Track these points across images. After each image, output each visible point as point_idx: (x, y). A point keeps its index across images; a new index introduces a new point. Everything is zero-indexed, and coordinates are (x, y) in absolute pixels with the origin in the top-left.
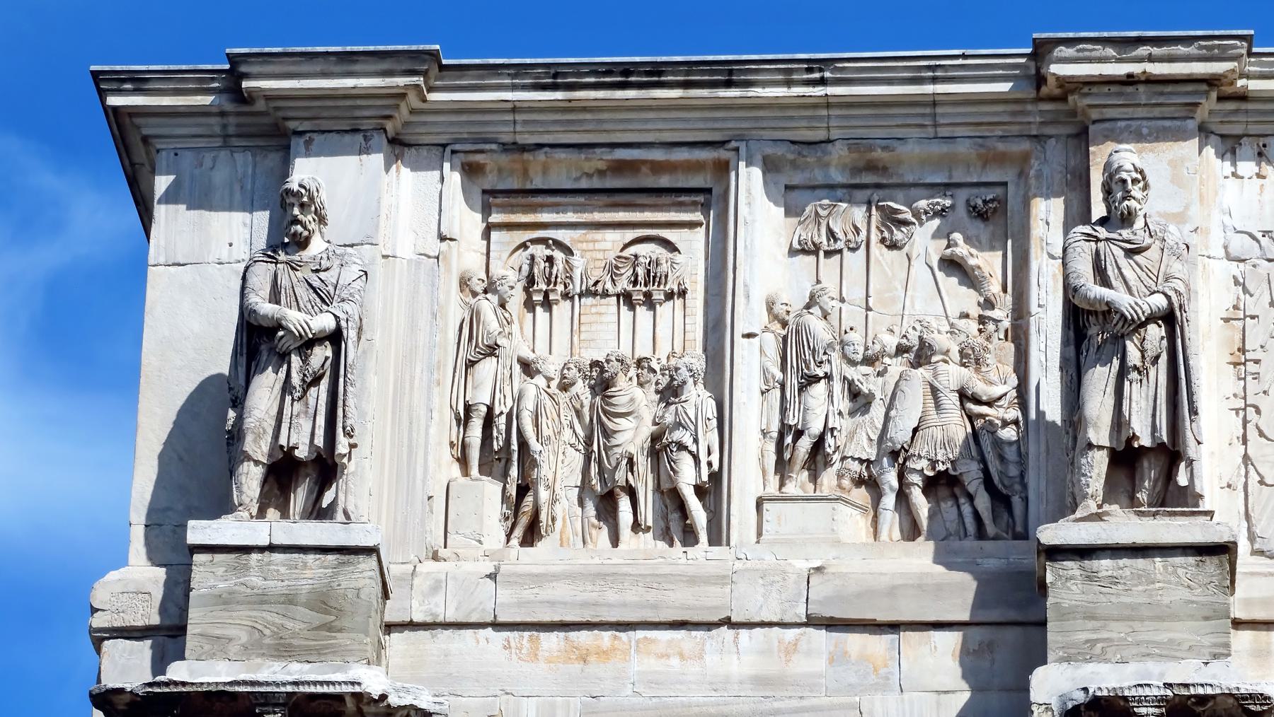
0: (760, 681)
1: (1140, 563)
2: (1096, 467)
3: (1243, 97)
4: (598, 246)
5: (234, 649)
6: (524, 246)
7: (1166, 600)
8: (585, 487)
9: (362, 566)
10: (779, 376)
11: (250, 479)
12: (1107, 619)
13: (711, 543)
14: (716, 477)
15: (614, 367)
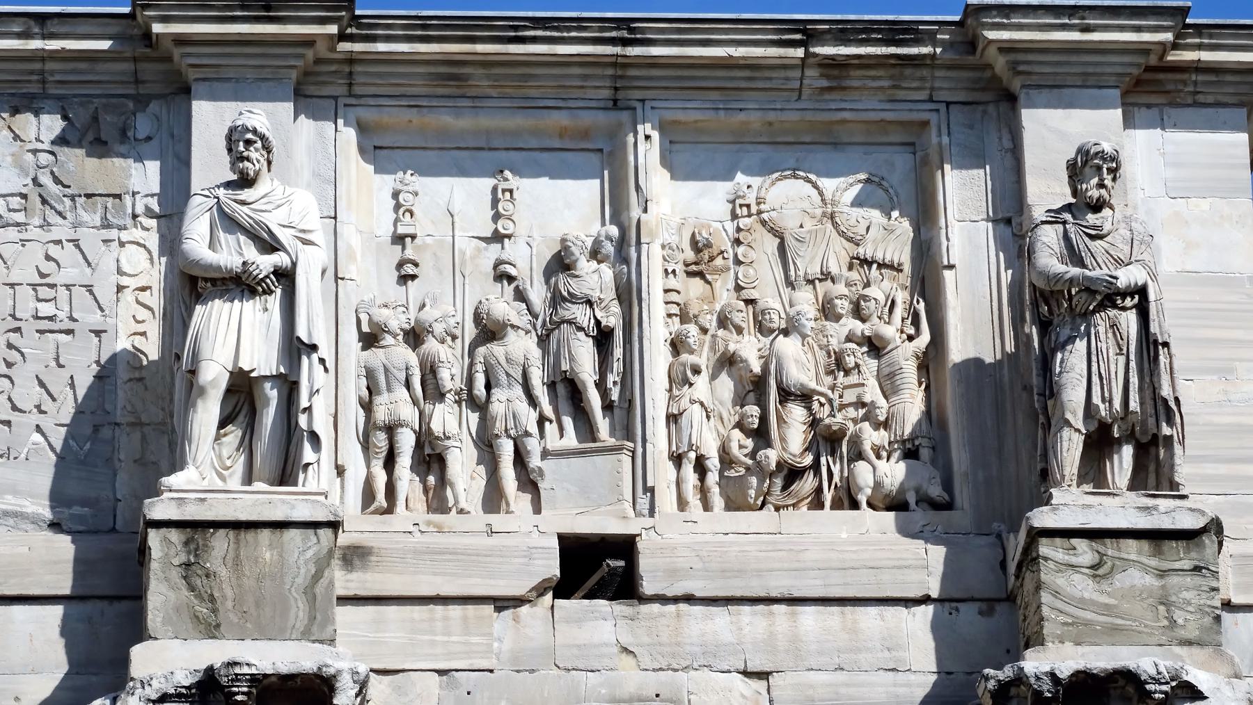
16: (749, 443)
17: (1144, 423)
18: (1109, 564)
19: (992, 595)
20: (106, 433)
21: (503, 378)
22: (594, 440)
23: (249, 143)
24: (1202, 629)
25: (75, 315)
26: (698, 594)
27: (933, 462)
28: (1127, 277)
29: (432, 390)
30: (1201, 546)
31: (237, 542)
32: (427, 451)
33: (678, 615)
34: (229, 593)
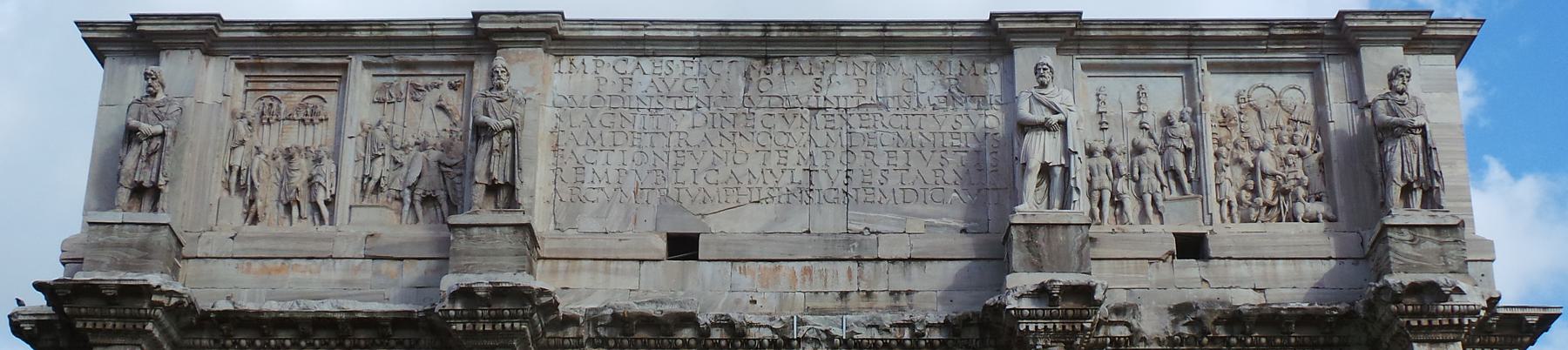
0: (343, 282)
1: (490, 231)
2: (479, 191)
3: (563, 39)
4: (293, 99)
5: (104, 266)
6: (261, 99)
7: (500, 248)
8: (279, 200)
9: (162, 232)
10: (363, 154)
11: (124, 195)
12: (474, 255)
13: (330, 225)
14: (333, 196)
15: (293, 151)
16: (1249, 195)
17: (1426, 182)
18: (1418, 240)
19: (1359, 256)
20: (983, 192)
21: (1146, 170)
22: (1185, 194)
23: (1044, 69)
24: (1460, 266)
25: (969, 145)
26: (1234, 257)
27: (1328, 202)
28: (1418, 121)
29: (1117, 173)
30: (1457, 231)
31: (1049, 232)
32: (1116, 199)
33: (1226, 266)
34: (1046, 254)
